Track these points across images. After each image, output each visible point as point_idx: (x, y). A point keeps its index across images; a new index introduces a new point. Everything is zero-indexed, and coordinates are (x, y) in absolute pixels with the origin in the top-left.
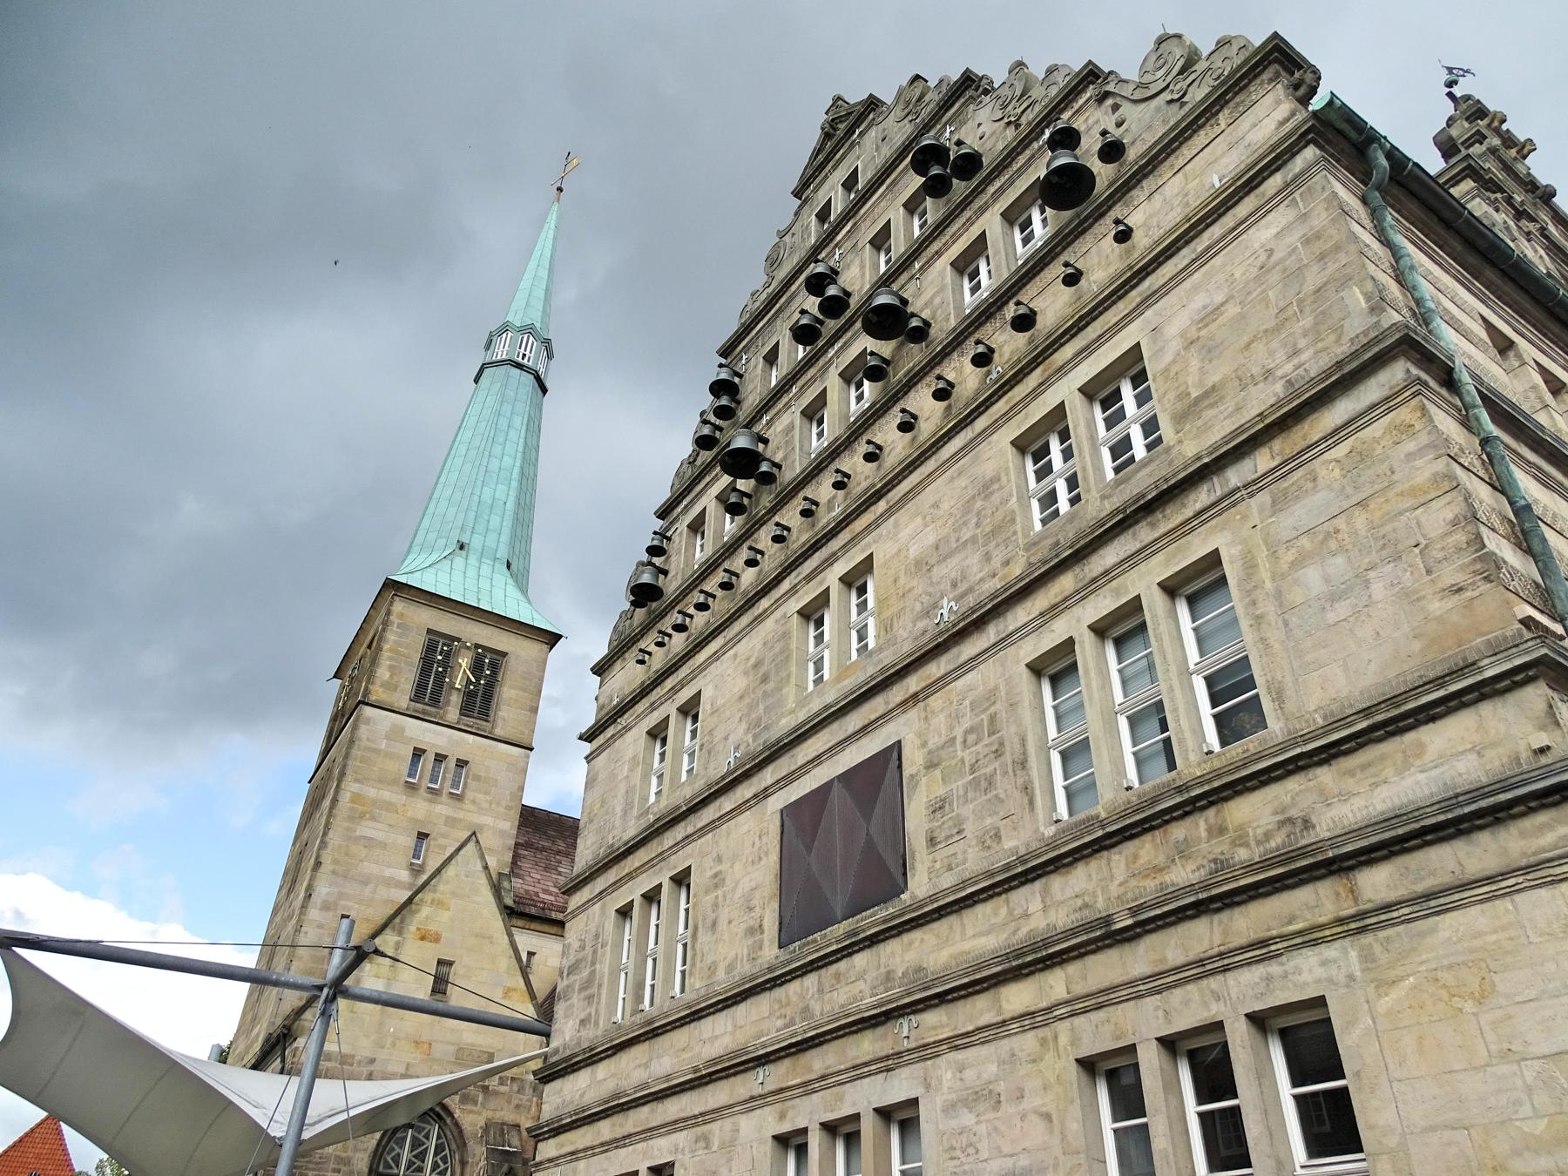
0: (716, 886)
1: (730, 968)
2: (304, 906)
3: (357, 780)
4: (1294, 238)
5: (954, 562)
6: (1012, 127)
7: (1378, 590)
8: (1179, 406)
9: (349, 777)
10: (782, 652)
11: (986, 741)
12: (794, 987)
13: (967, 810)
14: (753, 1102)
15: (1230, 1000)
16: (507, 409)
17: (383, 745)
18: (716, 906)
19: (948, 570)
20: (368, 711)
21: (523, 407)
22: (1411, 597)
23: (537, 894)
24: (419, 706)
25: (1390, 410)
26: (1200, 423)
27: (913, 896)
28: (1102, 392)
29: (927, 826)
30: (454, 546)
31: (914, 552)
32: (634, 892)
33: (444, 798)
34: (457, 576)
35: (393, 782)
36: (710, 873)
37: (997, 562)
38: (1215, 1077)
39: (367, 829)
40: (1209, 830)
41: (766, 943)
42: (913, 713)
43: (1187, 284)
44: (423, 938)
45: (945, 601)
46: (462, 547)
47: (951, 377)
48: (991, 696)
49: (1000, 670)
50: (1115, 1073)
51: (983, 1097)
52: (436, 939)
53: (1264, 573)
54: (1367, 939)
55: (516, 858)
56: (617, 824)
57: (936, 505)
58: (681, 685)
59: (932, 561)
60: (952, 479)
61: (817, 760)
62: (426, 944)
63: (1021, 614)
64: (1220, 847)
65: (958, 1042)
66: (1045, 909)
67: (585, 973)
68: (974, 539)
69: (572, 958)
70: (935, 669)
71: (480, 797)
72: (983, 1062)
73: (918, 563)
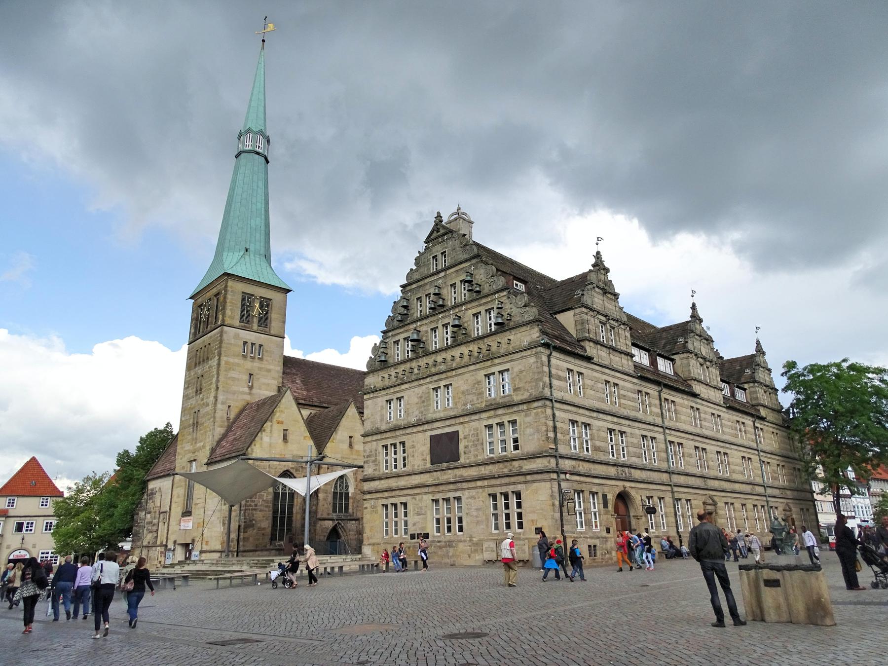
2: (215, 404)
12: (435, 473)
14: (426, 493)
15: (510, 489)
17: (233, 341)
19: (470, 397)
21: (262, 176)
22: (538, 439)
30: (244, 250)
31: (462, 389)
33: (256, 360)
35: (238, 356)
38: (506, 496)
39: (232, 374)
42: (461, 426)
48: (477, 429)
49: (478, 424)
50: (494, 497)
61: (439, 428)
63: (484, 415)
65: (468, 489)
70: (466, 419)
72: (473, 492)
73: (463, 393)
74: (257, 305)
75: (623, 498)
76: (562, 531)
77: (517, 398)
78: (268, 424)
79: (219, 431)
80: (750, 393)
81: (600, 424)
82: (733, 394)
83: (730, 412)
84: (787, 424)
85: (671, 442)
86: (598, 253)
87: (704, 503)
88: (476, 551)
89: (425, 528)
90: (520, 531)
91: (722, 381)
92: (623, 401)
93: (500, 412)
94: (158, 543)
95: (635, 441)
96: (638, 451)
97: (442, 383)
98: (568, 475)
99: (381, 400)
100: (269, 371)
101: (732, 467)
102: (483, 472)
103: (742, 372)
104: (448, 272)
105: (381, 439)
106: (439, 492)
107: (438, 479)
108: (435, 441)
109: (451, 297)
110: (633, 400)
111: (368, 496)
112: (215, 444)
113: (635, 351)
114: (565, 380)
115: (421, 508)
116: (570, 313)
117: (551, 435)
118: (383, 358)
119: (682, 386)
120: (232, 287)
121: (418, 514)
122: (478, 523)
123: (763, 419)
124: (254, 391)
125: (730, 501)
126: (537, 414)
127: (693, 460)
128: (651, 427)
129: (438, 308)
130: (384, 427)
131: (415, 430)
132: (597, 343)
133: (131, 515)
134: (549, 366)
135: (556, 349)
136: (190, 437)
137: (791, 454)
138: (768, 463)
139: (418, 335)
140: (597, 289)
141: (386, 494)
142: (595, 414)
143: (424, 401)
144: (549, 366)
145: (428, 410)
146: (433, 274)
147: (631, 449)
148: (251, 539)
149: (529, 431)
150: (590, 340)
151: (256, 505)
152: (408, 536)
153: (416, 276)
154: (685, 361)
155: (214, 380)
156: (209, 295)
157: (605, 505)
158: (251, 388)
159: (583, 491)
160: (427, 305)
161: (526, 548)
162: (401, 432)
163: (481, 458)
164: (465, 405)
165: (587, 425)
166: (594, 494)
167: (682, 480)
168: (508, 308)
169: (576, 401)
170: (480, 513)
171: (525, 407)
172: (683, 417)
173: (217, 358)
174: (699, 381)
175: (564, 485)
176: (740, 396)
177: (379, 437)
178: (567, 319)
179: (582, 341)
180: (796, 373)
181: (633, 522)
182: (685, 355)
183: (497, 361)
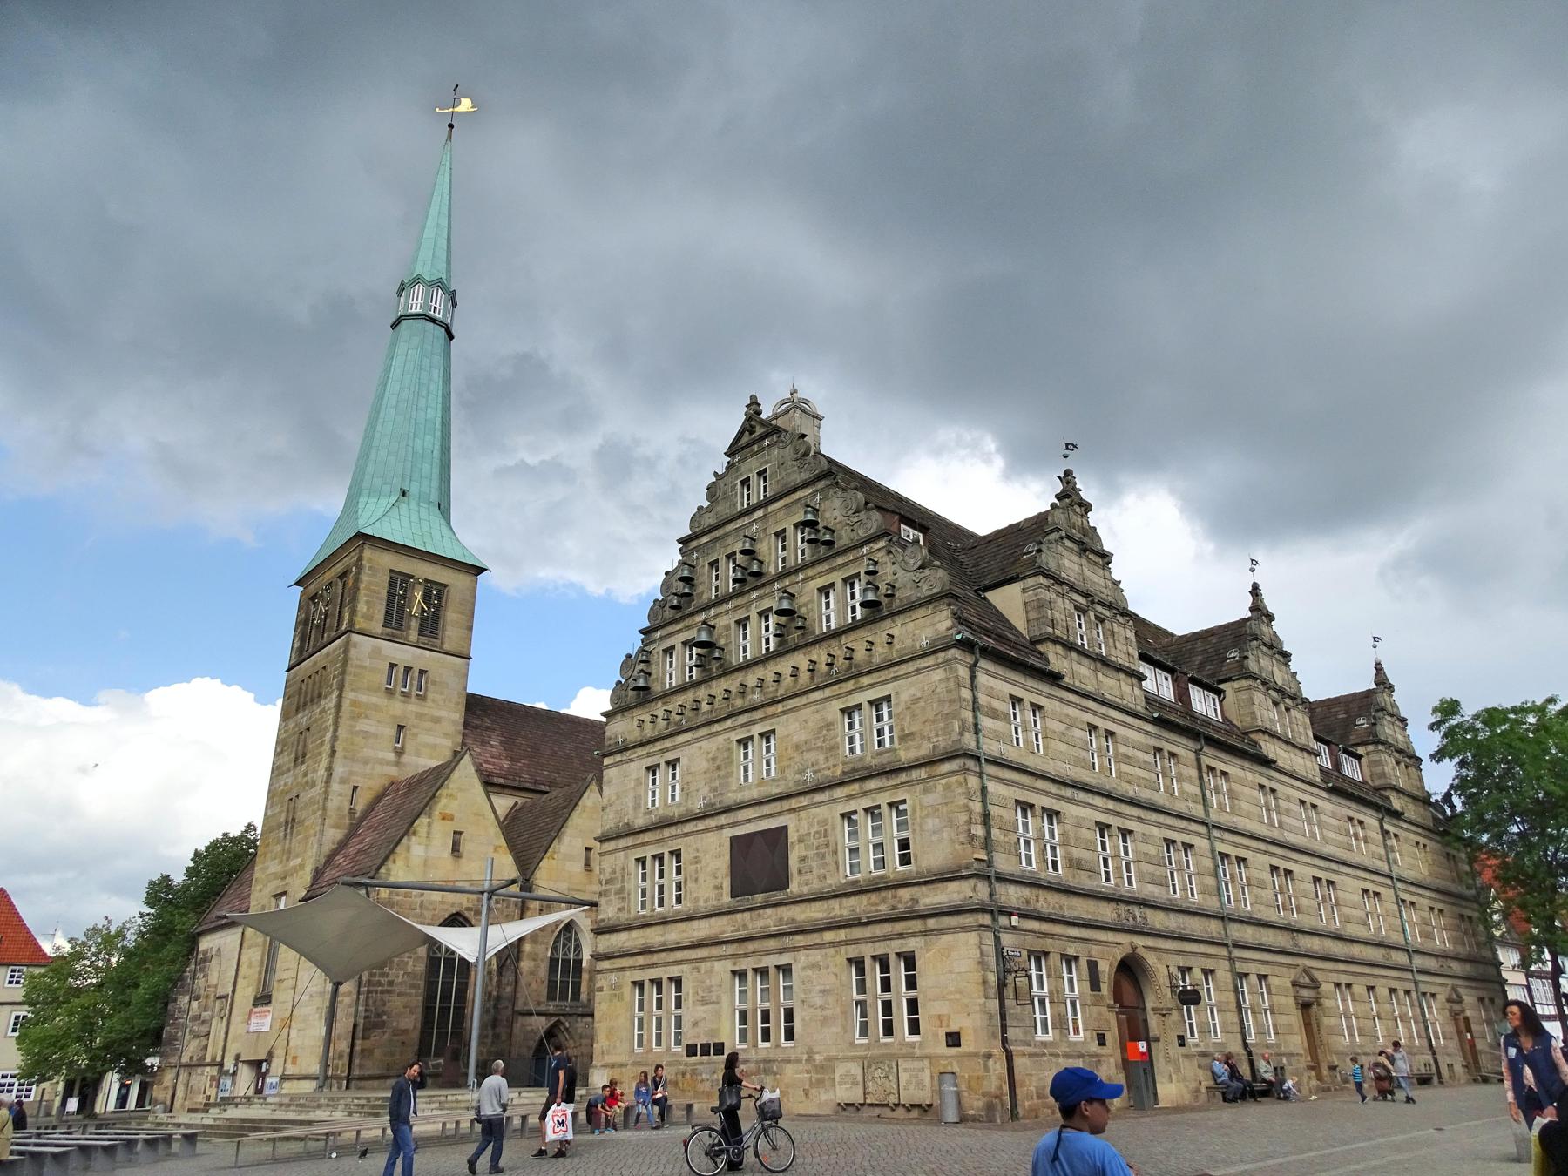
1: (706, 901)
9: (347, 688)
12: (739, 916)
13: (814, 864)
14: (720, 958)
15: (891, 948)
16: (426, 362)
17: (367, 663)
19: (811, 756)
20: (355, 637)
21: (438, 360)
22: (952, 841)
30: (398, 493)
31: (795, 739)
33: (413, 699)
34: (405, 520)
35: (377, 690)
37: (831, 763)
38: (885, 968)
39: (363, 725)
42: (793, 816)
46: (404, 494)
48: (825, 822)
49: (827, 810)
50: (859, 964)
51: (814, 966)
52: (452, 818)
55: (464, 735)
61: (748, 821)
63: (839, 793)
64: (891, 902)
65: (806, 948)
69: (608, 876)
70: (804, 801)
71: (437, 697)
72: (816, 956)
73: (797, 747)
74: (419, 595)
75: (1131, 969)
76: (1004, 1041)
77: (906, 755)
78: (423, 820)
79: (333, 835)
80: (1370, 764)
81: (1081, 812)
82: (1337, 765)
83: (1334, 798)
84: (1442, 828)
85: (1224, 856)
86: (1068, 473)
87: (1295, 984)
88: (820, 1082)
89: (714, 1032)
90: (915, 1039)
91: (1317, 738)
92: (1125, 768)
93: (872, 784)
94: (208, 1060)
95: (1152, 850)
96: (1159, 871)
97: (757, 730)
98: (1014, 919)
99: (636, 768)
100: (437, 720)
101: (1346, 910)
102: (837, 912)
103: (1353, 721)
104: (771, 508)
105: (634, 846)
106: (746, 955)
107: (745, 927)
108: (740, 845)
109: (774, 556)
110: (1144, 766)
111: (605, 965)
112: (323, 860)
113: (1145, 669)
114: (1005, 717)
115: (709, 989)
116: (1015, 588)
117: (979, 831)
118: (641, 683)
119: (1239, 745)
120: (370, 560)
121: (704, 1002)
122: (825, 1021)
123: (1398, 815)
124: (406, 758)
125: (1344, 979)
126: (948, 787)
127: (1268, 894)
128: (1183, 824)
129: (751, 579)
130: (640, 821)
131: (701, 825)
132: (1069, 647)
133: (163, 1001)
134: (973, 687)
135: (987, 653)
136: (278, 848)
137: (1453, 888)
138: (1412, 903)
139: (710, 634)
140: (1068, 543)
141: (640, 960)
142: (1068, 792)
143: (720, 765)
144: (973, 687)
145: (727, 785)
146: (742, 515)
147: (1146, 867)
148: (377, 1053)
149: (931, 823)
150: (1056, 641)
151: (391, 983)
152: (681, 1049)
153: (709, 520)
154: (1244, 696)
155: (329, 735)
156: (330, 575)
157: (1095, 984)
158: (400, 752)
159: (1046, 954)
160: (729, 572)
161: (926, 1077)
162: (673, 831)
163: (832, 882)
164: (802, 772)
165: (1052, 814)
166: (1070, 960)
167: (1249, 934)
168: (887, 572)
169: (1031, 762)
170: (831, 999)
171: (923, 773)
172: (1244, 806)
173: (336, 693)
174: (1273, 735)
175: (1007, 939)
176: (1351, 769)
177: (630, 841)
178: (1009, 601)
179: (1041, 641)
180: (1459, 725)
181: (1154, 1021)
182: (1244, 683)
183: (865, 680)
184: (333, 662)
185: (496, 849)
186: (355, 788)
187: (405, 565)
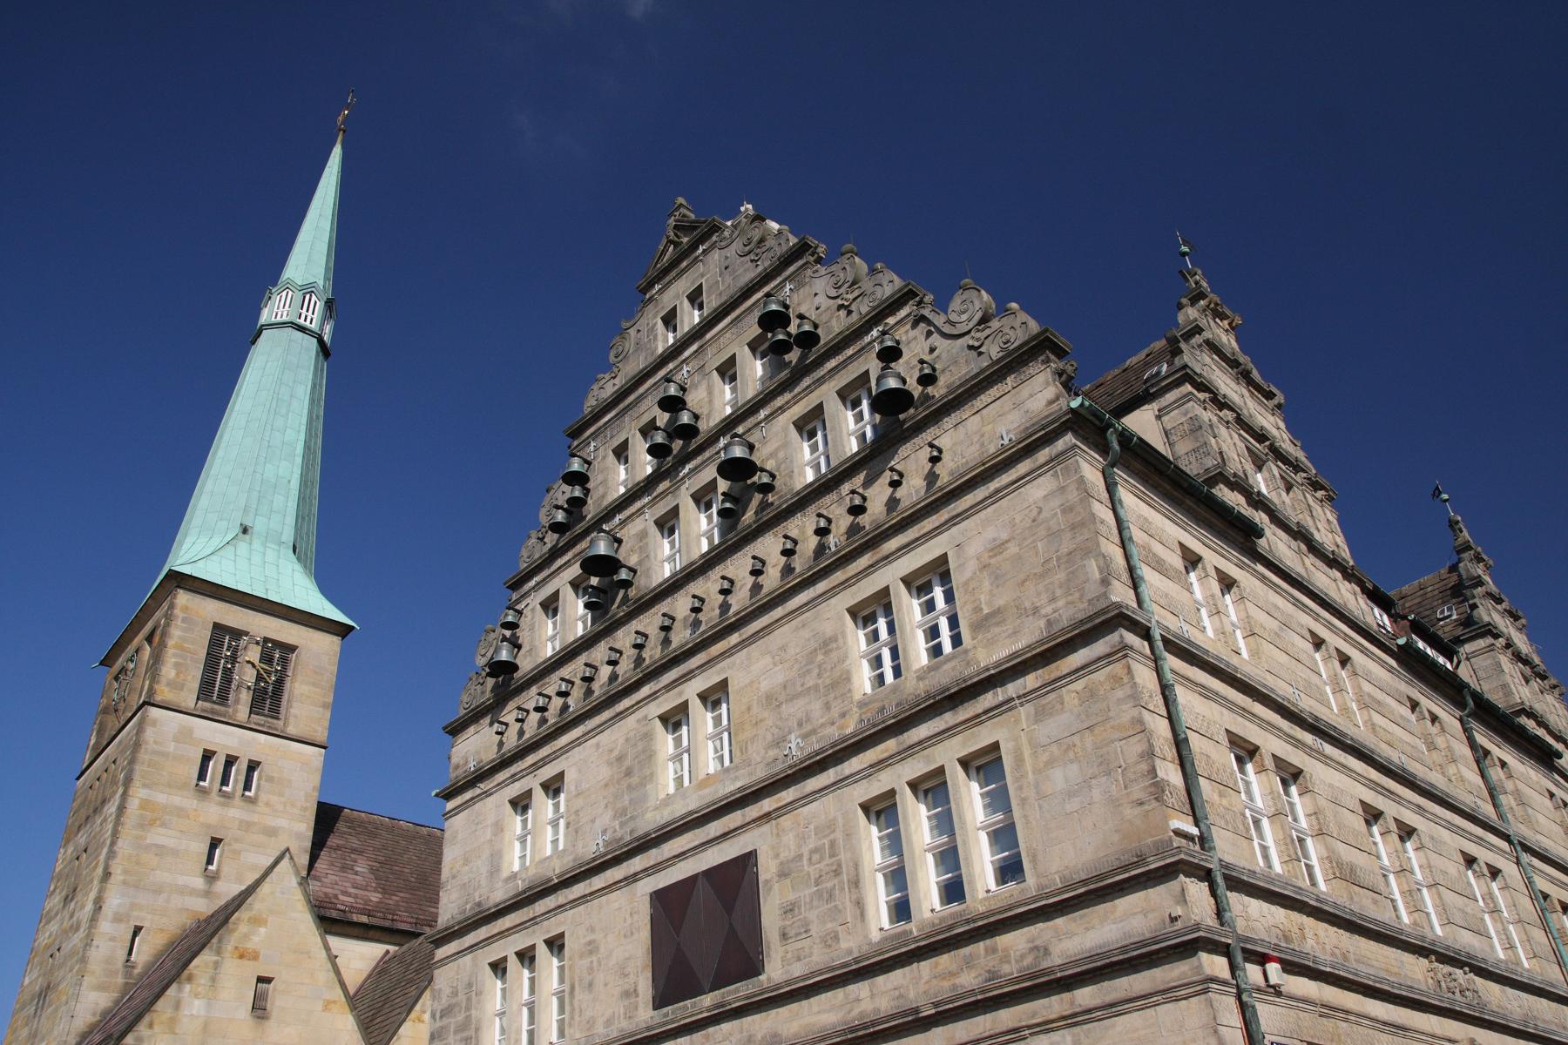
0: (591, 952)
1: (608, 1023)
2: (94, 920)
3: (145, 786)
4: (1055, 503)
5: (801, 702)
6: (843, 313)
7: (1096, 794)
8: (974, 617)
10: (644, 751)
11: (827, 861)
13: (812, 915)
17: (171, 747)
18: (591, 970)
19: (794, 710)
22: (1114, 803)
23: (336, 896)
24: (208, 705)
25: (1110, 663)
26: (989, 636)
27: (769, 979)
28: (919, 584)
29: (780, 924)
30: (238, 530)
31: (765, 686)
32: (508, 949)
33: (237, 800)
36: (583, 941)
37: (835, 712)
39: (158, 836)
40: (986, 950)
41: (641, 1006)
42: (766, 828)
43: (982, 514)
44: (241, 957)
45: (793, 737)
46: (245, 531)
47: (794, 533)
48: (831, 826)
49: (835, 805)
52: (255, 956)
53: (1028, 767)
54: (1076, 1030)
56: (484, 882)
57: (783, 648)
58: (544, 762)
59: (782, 698)
60: (797, 628)
61: (682, 856)
62: (245, 962)
64: (991, 962)
66: (872, 996)
67: (461, 1017)
68: (816, 688)
69: (444, 1002)
70: (788, 795)
71: (274, 799)
73: (769, 698)
109: (714, 401)
118: (504, 655)
126: (1091, 694)
149: (1059, 778)
158: (212, 878)
163: (850, 947)
164: (779, 742)
182: (1481, 643)
184: (123, 752)
185: (327, 1005)
186: (137, 930)
187: (235, 617)
